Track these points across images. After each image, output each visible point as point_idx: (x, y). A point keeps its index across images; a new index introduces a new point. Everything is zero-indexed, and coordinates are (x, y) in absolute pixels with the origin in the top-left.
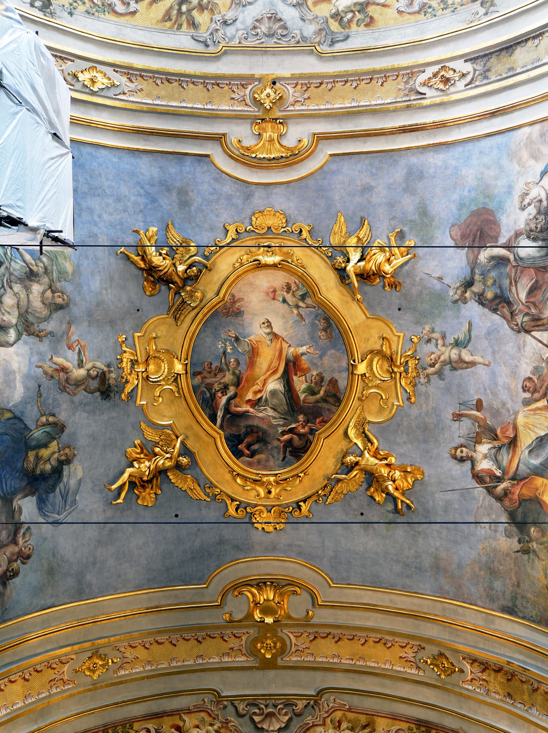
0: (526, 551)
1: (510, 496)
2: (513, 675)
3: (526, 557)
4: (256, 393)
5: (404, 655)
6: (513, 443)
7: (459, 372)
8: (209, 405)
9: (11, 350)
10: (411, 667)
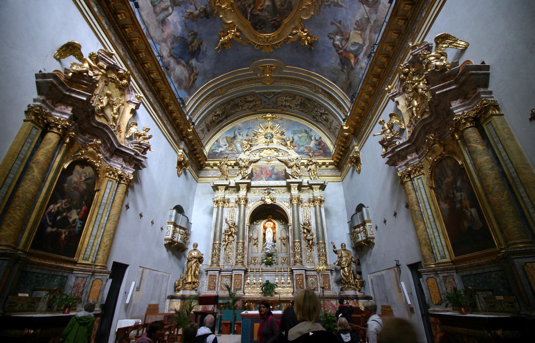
0: (343, 71)
4: (261, 6)
6: (347, 40)
7: (336, 7)
8: (244, 13)
9: (172, 15)
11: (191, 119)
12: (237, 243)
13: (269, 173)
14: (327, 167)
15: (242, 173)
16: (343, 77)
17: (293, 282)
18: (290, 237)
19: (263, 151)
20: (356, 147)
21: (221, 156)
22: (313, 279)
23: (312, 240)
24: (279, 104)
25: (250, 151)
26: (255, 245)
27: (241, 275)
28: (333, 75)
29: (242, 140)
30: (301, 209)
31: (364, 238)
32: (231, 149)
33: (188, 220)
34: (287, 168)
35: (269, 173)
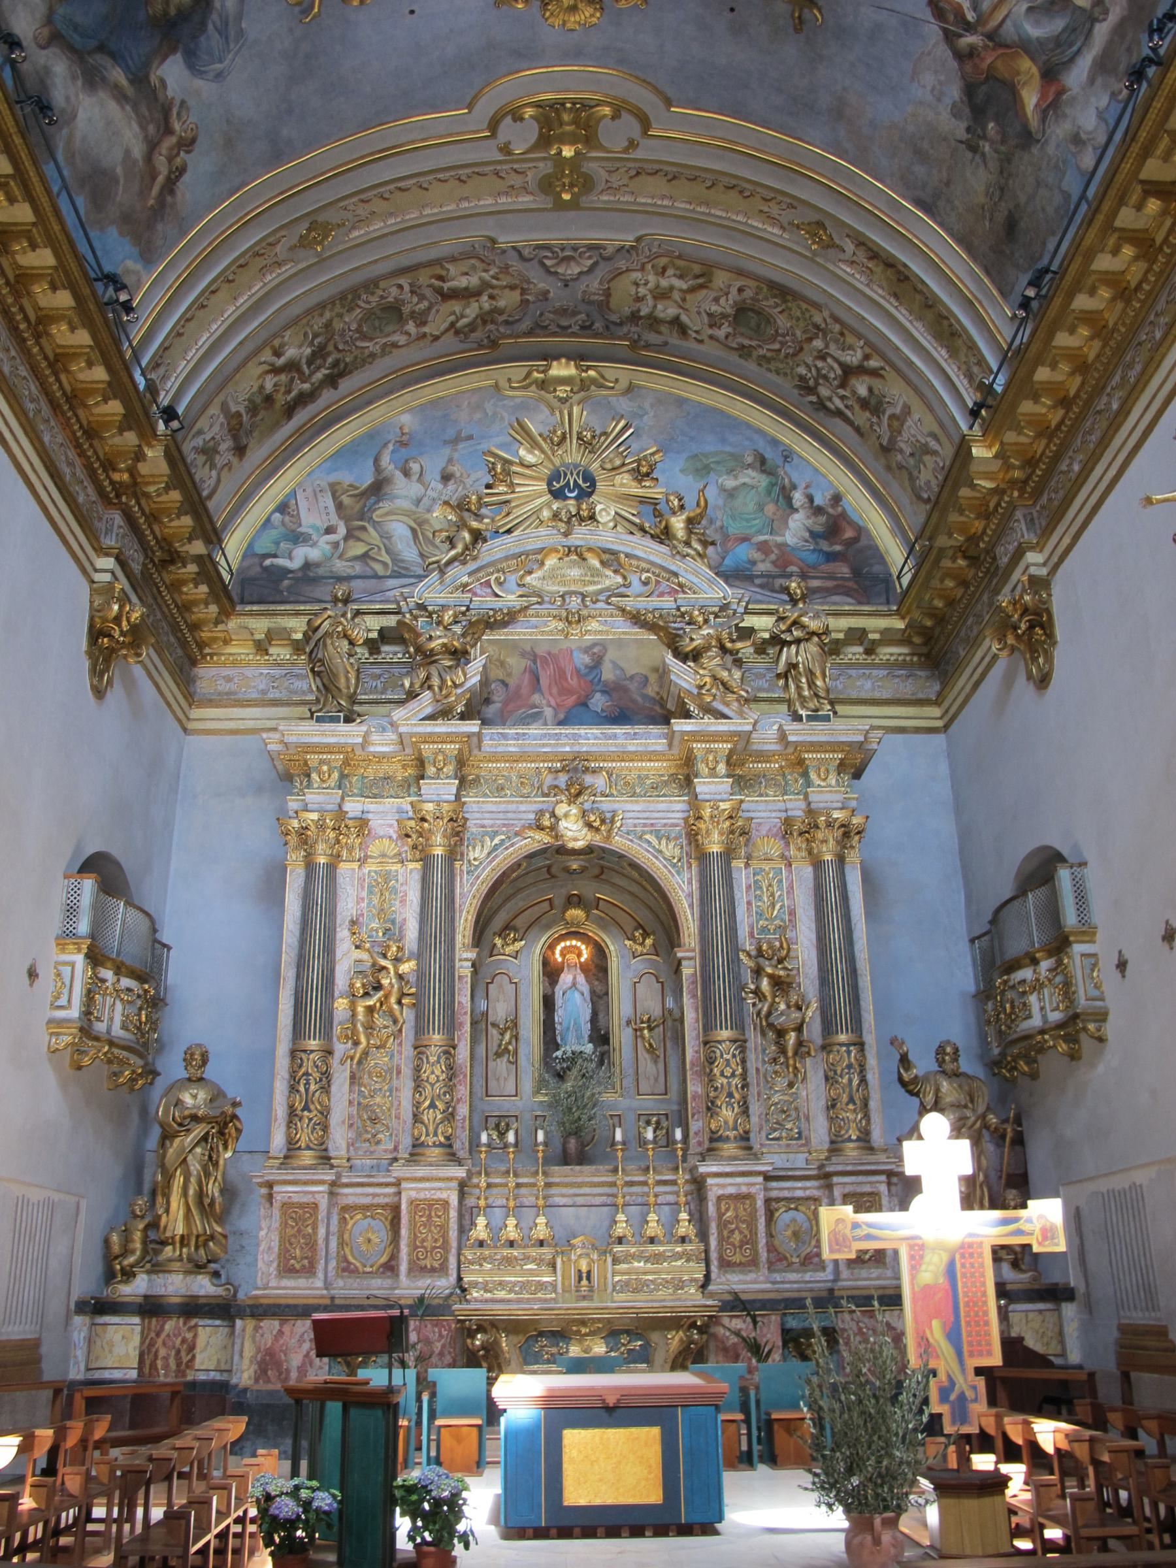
0: (974, 149)
1: (976, 60)
2: (907, 278)
3: (969, 155)
5: (766, 209)
10: (773, 225)
11: (152, 388)
12: (419, 1048)
13: (574, 682)
14: (869, 652)
15: (436, 681)
16: (977, 180)
17: (703, 1236)
18: (690, 1016)
19: (542, 564)
20: (1032, 557)
21: (308, 590)
22: (800, 1217)
23: (799, 1029)
24: (622, 305)
25: (472, 566)
26: (498, 1055)
27: (446, 1204)
28: (919, 170)
29: (418, 501)
30: (742, 876)
31: (1055, 1017)
32: (359, 549)
33: (155, 931)
34: (670, 658)
35: (574, 682)
